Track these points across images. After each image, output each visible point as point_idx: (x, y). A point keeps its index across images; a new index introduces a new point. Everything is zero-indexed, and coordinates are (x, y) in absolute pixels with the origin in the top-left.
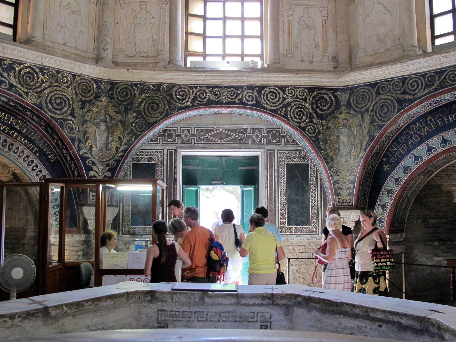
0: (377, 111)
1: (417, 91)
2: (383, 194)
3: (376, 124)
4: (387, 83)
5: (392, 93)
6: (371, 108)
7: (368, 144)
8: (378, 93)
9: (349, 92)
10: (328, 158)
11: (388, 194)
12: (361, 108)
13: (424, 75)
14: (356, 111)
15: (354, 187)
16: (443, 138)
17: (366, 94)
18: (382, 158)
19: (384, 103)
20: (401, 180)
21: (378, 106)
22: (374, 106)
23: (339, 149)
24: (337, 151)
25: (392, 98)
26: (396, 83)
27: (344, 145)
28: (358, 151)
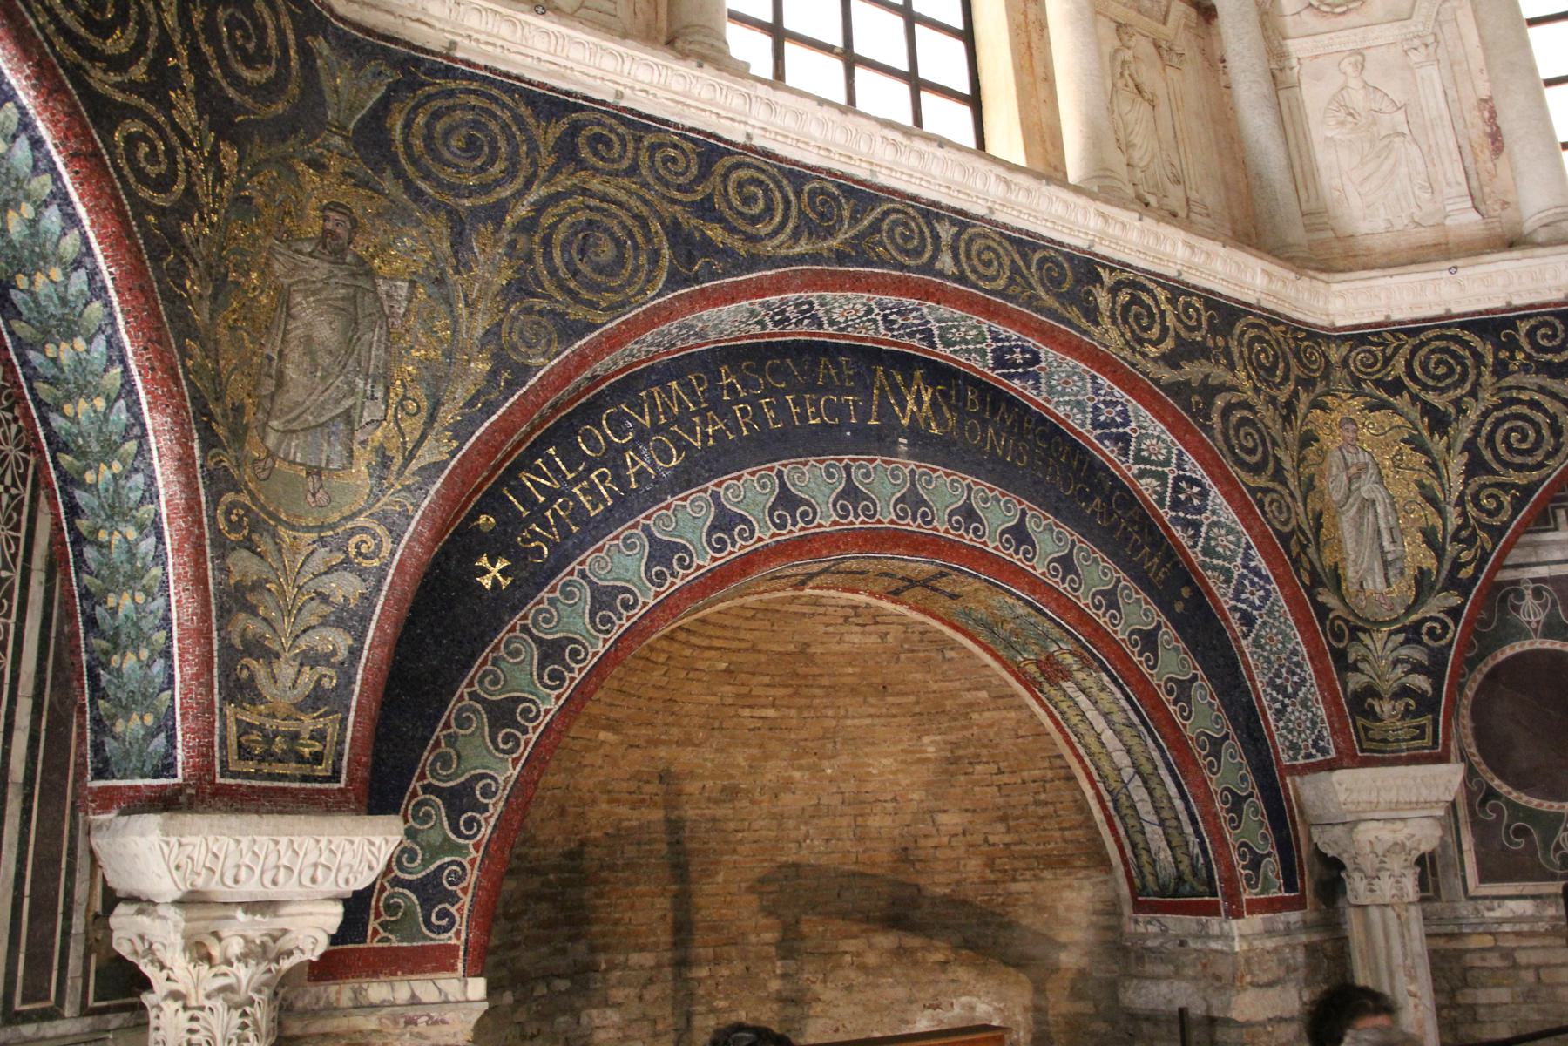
0: (559, 237)
1: (762, 229)
2: (463, 723)
3: (546, 304)
4: (622, 130)
5: (645, 185)
6: (523, 211)
7: (479, 404)
8: (567, 152)
9: (392, 76)
10: (217, 410)
11: (495, 726)
12: (455, 190)
13: (797, 174)
14: (418, 195)
15: (355, 653)
16: (783, 485)
17: (493, 126)
18: (474, 516)
19: (597, 216)
20: (575, 653)
21: (561, 218)
22: (540, 207)
23: (281, 374)
24: (269, 385)
25: (645, 211)
26: (672, 152)
27: (315, 364)
28: (412, 427)
